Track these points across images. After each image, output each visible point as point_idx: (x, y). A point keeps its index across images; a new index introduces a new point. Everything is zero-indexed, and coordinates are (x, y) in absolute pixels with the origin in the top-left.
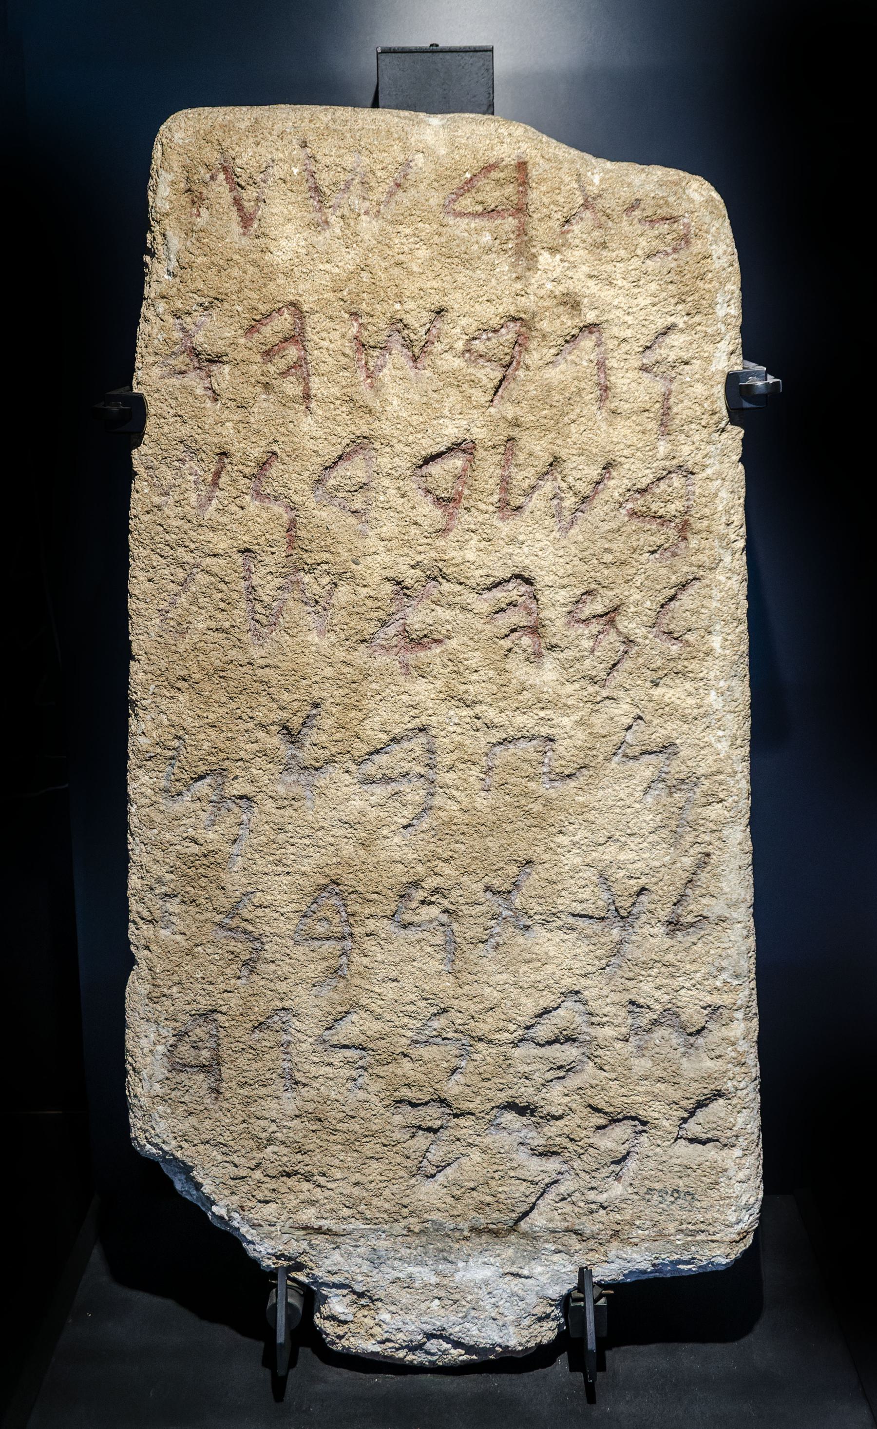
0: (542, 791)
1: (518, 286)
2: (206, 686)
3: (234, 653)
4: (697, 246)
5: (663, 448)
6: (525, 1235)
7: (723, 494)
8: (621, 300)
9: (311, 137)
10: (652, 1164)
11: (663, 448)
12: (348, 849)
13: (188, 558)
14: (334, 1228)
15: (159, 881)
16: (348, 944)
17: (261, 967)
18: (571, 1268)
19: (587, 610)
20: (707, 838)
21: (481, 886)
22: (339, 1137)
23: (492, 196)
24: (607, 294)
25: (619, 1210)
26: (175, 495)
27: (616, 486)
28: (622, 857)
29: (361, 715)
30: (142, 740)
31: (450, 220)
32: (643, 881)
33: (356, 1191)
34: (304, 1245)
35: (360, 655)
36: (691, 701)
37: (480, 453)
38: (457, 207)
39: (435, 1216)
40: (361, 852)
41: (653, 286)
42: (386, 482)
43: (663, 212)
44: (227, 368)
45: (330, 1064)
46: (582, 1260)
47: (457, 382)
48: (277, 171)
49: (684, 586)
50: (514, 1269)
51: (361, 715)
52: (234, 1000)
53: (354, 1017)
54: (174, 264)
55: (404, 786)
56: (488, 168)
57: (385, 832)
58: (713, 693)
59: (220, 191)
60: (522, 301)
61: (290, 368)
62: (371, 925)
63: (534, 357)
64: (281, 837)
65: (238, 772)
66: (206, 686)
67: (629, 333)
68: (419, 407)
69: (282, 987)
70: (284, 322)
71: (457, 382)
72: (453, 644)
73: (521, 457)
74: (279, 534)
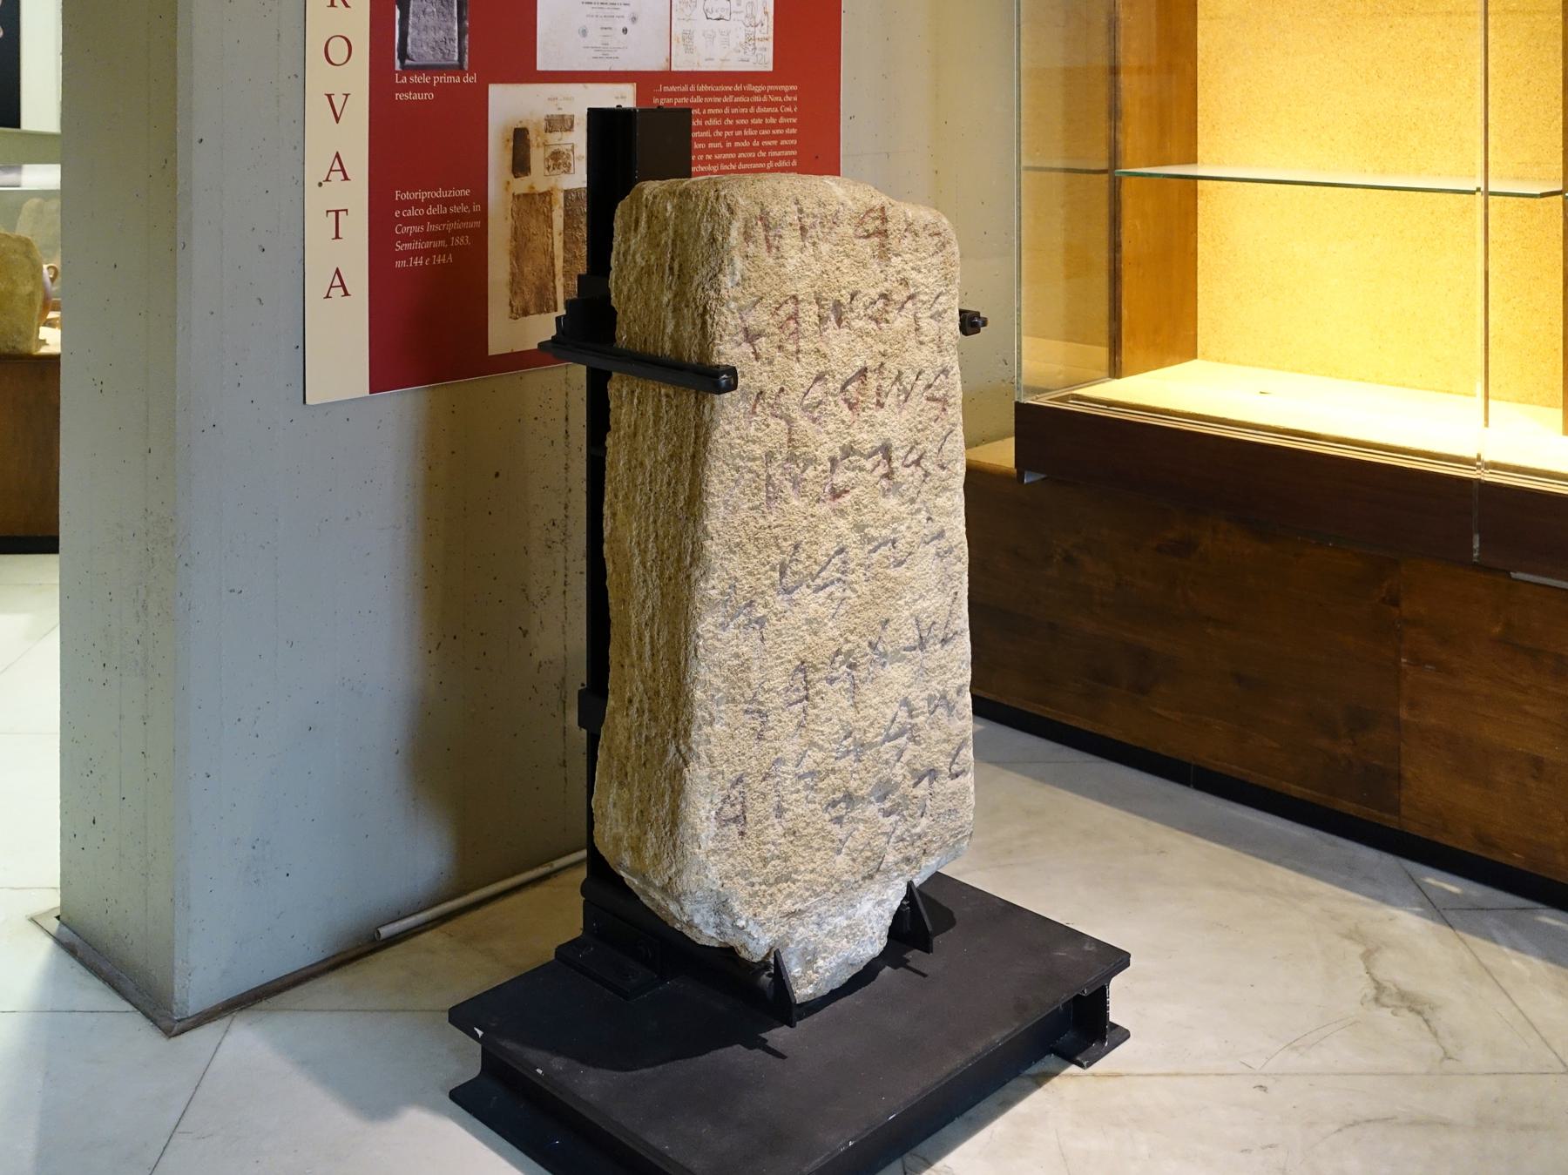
5: (939, 362)
23: (871, 228)
54: (738, 278)
55: (831, 589)
56: (871, 210)
59: (759, 232)
64: (779, 640)
68: (845, 349)
70: (790, 308)
71: (862, 334)
72: (856, 491)
74: (785, 440)
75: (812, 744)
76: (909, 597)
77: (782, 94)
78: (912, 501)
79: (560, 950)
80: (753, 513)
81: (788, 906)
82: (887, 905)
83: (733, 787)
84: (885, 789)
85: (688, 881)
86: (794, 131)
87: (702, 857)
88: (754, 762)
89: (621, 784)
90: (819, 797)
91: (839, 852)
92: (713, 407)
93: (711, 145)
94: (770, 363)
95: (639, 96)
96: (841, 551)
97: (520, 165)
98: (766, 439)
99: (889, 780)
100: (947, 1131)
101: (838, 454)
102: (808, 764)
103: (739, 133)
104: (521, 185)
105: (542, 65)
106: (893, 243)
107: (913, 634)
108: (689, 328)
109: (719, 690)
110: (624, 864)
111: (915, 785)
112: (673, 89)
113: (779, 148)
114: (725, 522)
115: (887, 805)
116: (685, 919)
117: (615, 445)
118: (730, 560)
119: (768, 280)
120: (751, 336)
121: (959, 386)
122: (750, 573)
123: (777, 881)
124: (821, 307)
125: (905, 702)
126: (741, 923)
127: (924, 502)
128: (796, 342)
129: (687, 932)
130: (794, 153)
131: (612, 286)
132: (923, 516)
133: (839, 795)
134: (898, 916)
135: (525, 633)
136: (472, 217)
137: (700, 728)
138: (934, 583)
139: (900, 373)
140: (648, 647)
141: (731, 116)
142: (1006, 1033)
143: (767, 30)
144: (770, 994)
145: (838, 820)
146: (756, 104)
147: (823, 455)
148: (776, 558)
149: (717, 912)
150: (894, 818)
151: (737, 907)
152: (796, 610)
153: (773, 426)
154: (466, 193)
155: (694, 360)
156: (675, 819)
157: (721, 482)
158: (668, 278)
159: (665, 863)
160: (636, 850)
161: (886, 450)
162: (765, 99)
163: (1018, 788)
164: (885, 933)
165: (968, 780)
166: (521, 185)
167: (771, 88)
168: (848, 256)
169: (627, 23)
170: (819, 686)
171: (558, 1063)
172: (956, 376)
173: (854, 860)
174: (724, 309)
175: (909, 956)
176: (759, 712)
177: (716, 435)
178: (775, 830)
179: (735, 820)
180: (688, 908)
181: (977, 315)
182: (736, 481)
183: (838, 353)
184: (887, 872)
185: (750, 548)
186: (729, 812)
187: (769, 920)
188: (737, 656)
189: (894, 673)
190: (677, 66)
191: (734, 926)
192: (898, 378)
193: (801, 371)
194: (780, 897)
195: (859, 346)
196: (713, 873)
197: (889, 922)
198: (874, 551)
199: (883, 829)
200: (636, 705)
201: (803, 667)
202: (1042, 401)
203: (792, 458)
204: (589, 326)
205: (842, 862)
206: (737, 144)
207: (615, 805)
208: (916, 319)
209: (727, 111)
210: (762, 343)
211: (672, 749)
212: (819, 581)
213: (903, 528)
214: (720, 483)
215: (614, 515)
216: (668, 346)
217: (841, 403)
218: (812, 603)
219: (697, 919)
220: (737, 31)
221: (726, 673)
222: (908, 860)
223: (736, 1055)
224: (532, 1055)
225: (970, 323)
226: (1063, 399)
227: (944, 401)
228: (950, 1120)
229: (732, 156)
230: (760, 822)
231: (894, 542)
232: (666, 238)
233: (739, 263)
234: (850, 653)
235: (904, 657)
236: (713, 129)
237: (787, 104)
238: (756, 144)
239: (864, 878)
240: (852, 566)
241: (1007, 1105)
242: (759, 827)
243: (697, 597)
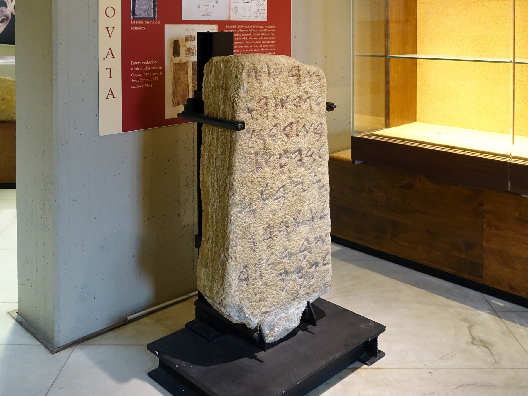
3: (254, 176)
5: (319, 120)
9: (268, 62)
23: (294, 73)
30: (236, 200)
37: (293, 125)
44: (255, 112)
54: (245, 90)
59: (253, 74)
64: (261, 217)
68: (284, 115)
70: (264, 101)
71: (291, 110)
74: (263, 147)
75: (273, 253)
76: (308, 202)
77: (270, 29)
78: (309, 169)
79: (187, 325)
80: (251, 173)
81: (264, 310)
82: (300, 309)
83: (244, 268)
84: (299, 269)
85: (228, 301)
86: (274, 42)
87: (233, 293)
88: (251, 260)
89: (206, 267)
90: (275, 272)
91: (283, 291)
92: (236, 136)
93: (245, 46)
94: (257, 120)
95: (218, 29)
96: (283, 186)
97: (176, 53)
98: (256, 147)
99: (301, 266)
100: (320, 387)
101: (282, 152)
102: (271, 260)
103: (254, 42)
104: (177, 60)
105: (183, 18)
106: (302, 78)
107: (309, 215)
108: (228, 108)
109: (239, 234)
110: (207, 294)
111: (310, 268)
112: (231, 27)
113: (269, 48)
114: (241, 176)
115: (300, 275)
116: (227, 314)
117: (204, 149)
118: (243, 189)
119: (256, 91)
120: (250, 111)
121: (326, 129)
122: (250, 194)
123: (260, 301)
124: (276, 101)
125: (307, 239)
126: (247, 316)
127: (313, 169)
128: (267, 113)
129: (229, 318)
130: (274, 49)
131: (203, 93)
132: (313, 174)
133: (283, 271)
134: (304, 313)
135: (179, 215)
136: (158, 71)
137: (232, 248)
138: (318, 198)
139: (305, 124)
140: (214, 220)
141: (252, 36)
142: (340, 354)
143: (265, 6)
144: (258, 340)
145: (282, 280)
146: (261, 32)
147: (277, 153)
148: (259, 189)
149: (239, 312)
150: (302, 279)
151: (245, 310)
152: (267, 207)
153: (258, 142)
154: (157, 62)
155: (230, 119)
156: (223, 279)
157: (239, 162)
158: (221, 90)
159: (220, 295)
160: (211, 290)
161: (300, 151)
162: (264, 31)
163: (350, 269)
164: (300, 319)
165: (330, 266)
166: (177, 60)
167: (266, 27)
168: (286, 83)
169: (215, 4)
170: (275, 233)
171: (183, 364)
172: (325, 126)
173: (288, 294)
174: (240, 101)
175: (308, 327)
176: (254, 242)
177: (237, 145)
178: (259, 283)
179: (245, 280)
180: (228, 310)
181: (333, 104)
182: (245, 162)
183: (282, 117)
184: (300, 298)
185: (250, 185)
186: (243, 277)
187: (257, 314)
189: (303, 229)
190: (233, 18)
191: (244, 316)
192: (304, 126)
193: (268, 123)
194: (261, 307)
195: (290, 115)
196: (237, 298)
197: (301, 315)
198: (295, 186)
199: (299, 283)
200: (211, 240)
201: (269, 227)
202: (361, 136)
203: (265, 154)
204: (195, 108)
205: (284, 294)
206: (254, 46)
207: (204, 274)
208: (311, 105)
209: (250, 34)
211: (223, 255)
212: (275, 197)
213: (306, 178)
214: (239, 162)
215: (203, 173)
216: (221, 114)
217: (283, 134)
218: (273, 204)
219: (232, 314)
220: (254, 6)
221: (241, 228)
222: (307, 294)
223: (245, 361)
224: (175, 360)
225: (330, 107)
226: (368, 135)
227: (321, 134)
228: (321, 384)
229: (252, 50)
230: (254, 280)
231: (302, 183)
232: (221, 76)
233: (246, 85)
234: (286, 222)
235: (306, 223)
236: (245, 41)
237: (272, 32)
238: (261, 46)
239: (292, 300)
240: (287, 191)
241: (341, 378)
242: (253, 282)
243: (231, 202)
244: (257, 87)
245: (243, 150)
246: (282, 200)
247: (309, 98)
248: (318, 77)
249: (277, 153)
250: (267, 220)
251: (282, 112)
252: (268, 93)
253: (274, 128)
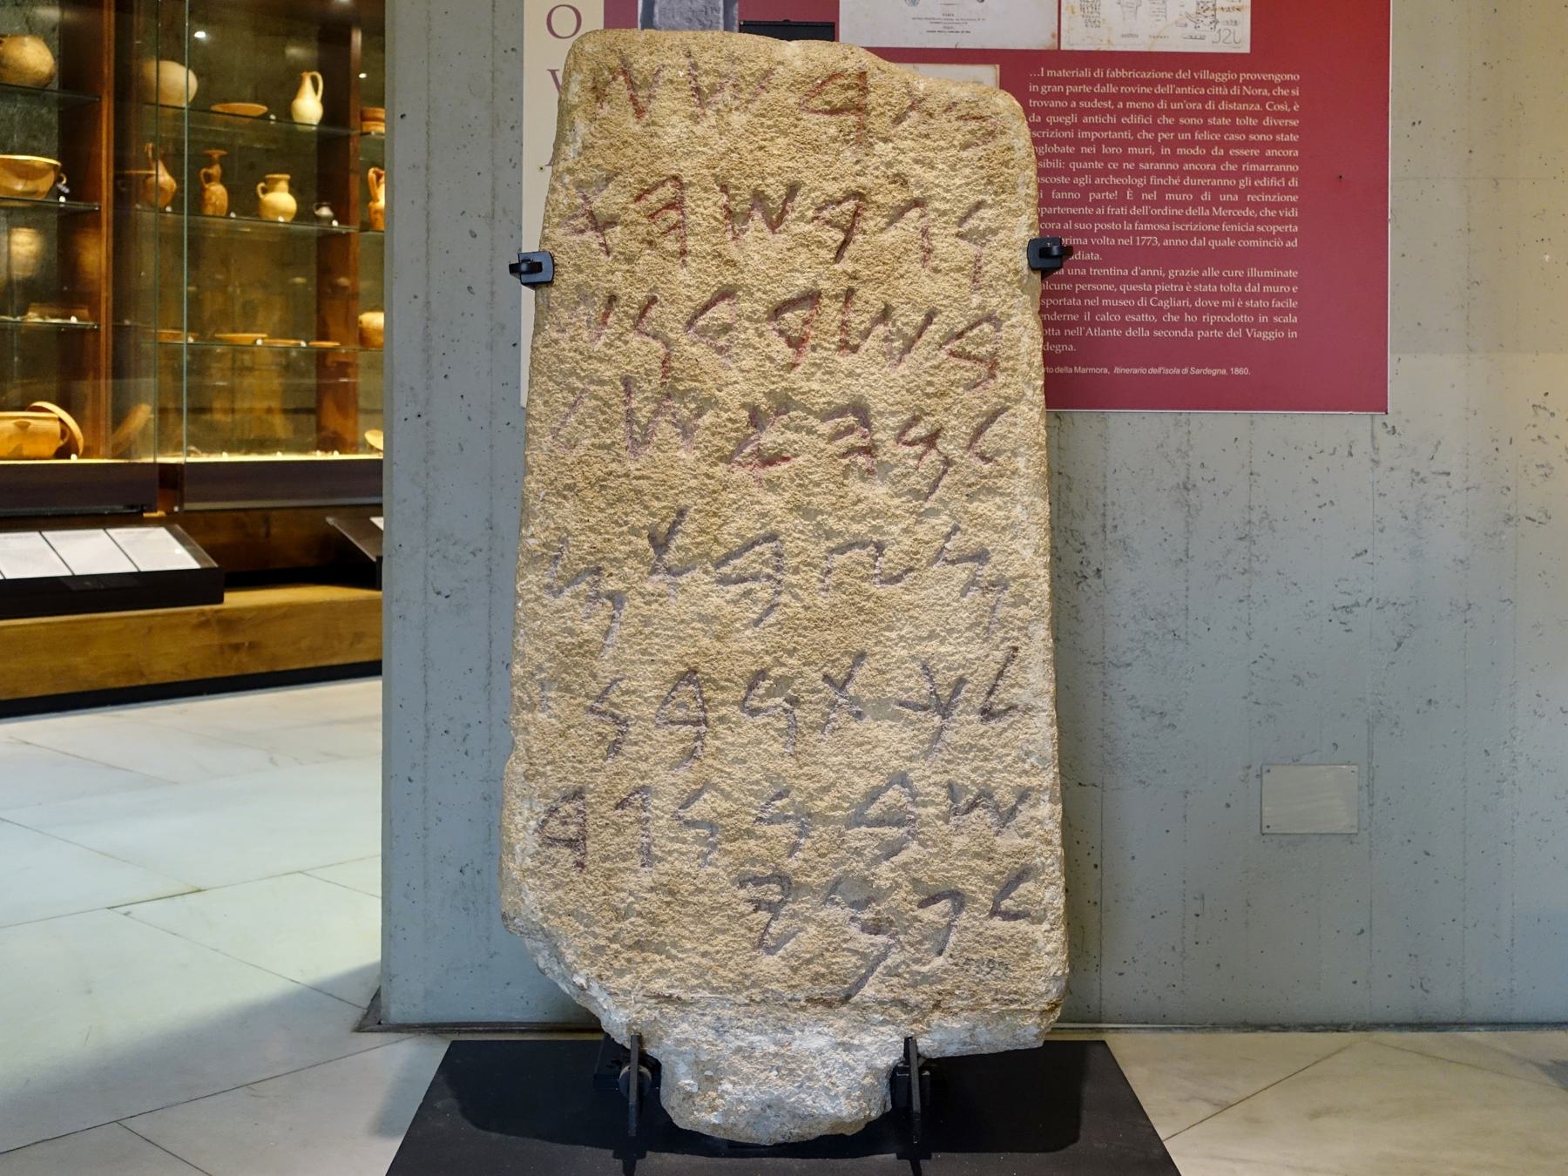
0: (873, 590)
1: (858, 167)
2: (589, 494)
3: (614, 466)
4: (1003, 141)
5: (976, 300)
6: (856, 1006)
7: (1025, 339)
8: (942, 181)
9: (694, 48)
10: (970, 936)
11: (976, 300)
12: (705, 642)
13: (579, 385)
14: (684, 996)
15: (540, 668)
16: (703, 728)
17: (626, 748)
18: (896, 1038)
19: (913, 433)
20: (1015, 634)
21: (820, 675)
22: (690, 910)
23: (838, 100)
24: (930, 176)
25: (941, 981)
26: (571, 332)
27: (934, 331)
28: (942, 649)
29: (719, 522)
30: (531, 541)
31: (805, 116)
32: (961, 672)
33: (704, 961)
34: (656, 1013)
35: (720, 470)
36: (1001, 513)
37: (826, 301)
38: (811, 106)
39: (774, 986)
40: (718, 644)
41: (967, 171)
42: (747, 324)
43: (975, 112)
44: (619, 228)
45: (684, 842)
46: (907, 1030)
47: (805, 242)
48: (666, 74)
49: (993, 417)
50: (845, 1039)
51: (719, 522)
52: (601, 779)
53: (706, 796)
55: (755, 586)
57: (738, 625)
58: (1019, 507)
59: (620, 86)
60: (861, 180)
61: (670, 229)
62: (723, 711)
63: (869, 225)
64: (647, 631)
65: (613, 570)
66: (589, 494)
67: (947, 206)
69: (643, 766)
70: (667, 192)
71: (805, 242)
72: (800, 460)
73: (859, 305)
74: (656, 365)
80: (601, 453)
96: (772, 537)
98: (620, 358)
106: (878, 124)
118: (558, 505)
120: (601, 224)
122: (591, 529)
124: (732, 198)
128: (682, 239)
147: (732, 397)
168: (786, 134)
188: (571, 632)
192: (885, 315)
198: (841, 550)
210: (616, 234)
244: (633, 135)
245: (562, 362)
246: (763, 591)
247: (917, 203)
248: (973, 125)
249: (732, 397)
250: (680, 649)
251: (758, 248)
252: (683, 164)
253: (723, 305)
